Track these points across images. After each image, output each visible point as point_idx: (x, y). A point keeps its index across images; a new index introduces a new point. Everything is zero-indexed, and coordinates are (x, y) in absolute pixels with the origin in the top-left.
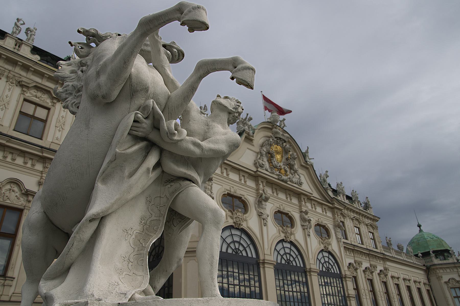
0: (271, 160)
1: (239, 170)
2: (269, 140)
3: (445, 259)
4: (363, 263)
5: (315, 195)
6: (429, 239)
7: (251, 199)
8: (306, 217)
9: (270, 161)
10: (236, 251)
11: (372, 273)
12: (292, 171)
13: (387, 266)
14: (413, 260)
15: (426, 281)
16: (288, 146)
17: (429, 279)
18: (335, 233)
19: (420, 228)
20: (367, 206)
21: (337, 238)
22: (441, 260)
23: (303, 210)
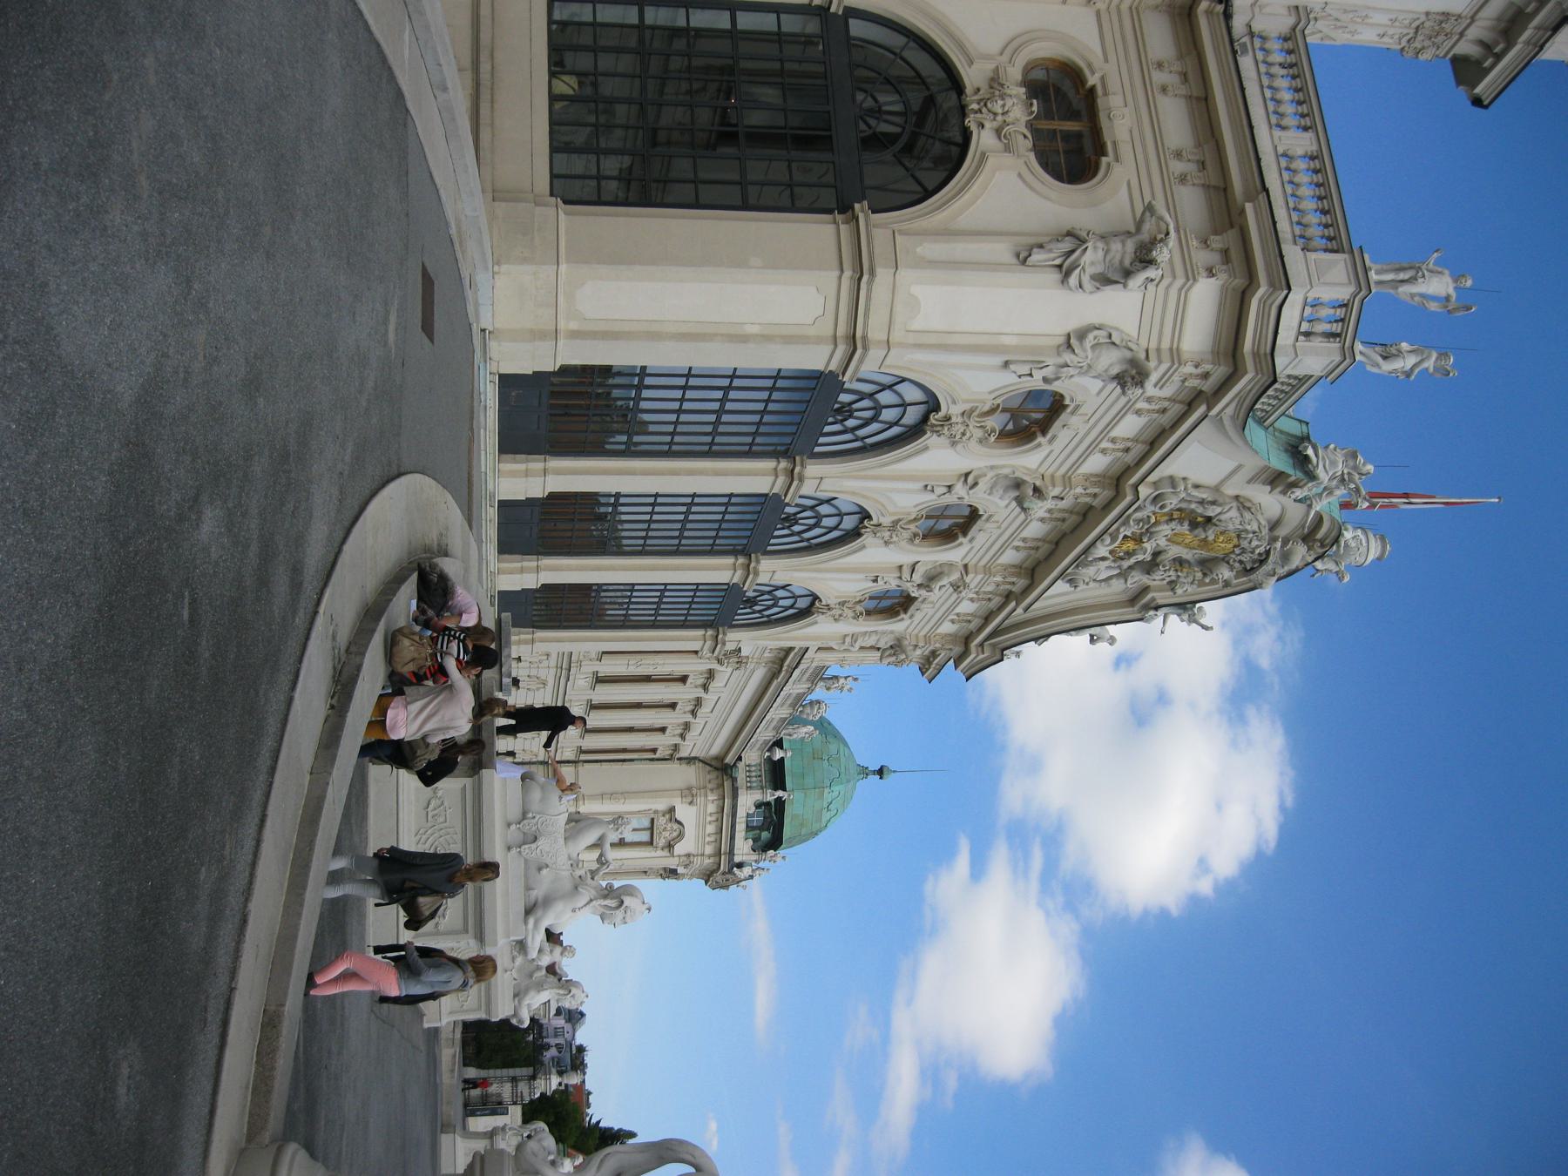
3: (749, 828)
6: (828, 796)
13: (750, 666)
17: (690, 760)
19: (874, 772)
23: (971, 576)
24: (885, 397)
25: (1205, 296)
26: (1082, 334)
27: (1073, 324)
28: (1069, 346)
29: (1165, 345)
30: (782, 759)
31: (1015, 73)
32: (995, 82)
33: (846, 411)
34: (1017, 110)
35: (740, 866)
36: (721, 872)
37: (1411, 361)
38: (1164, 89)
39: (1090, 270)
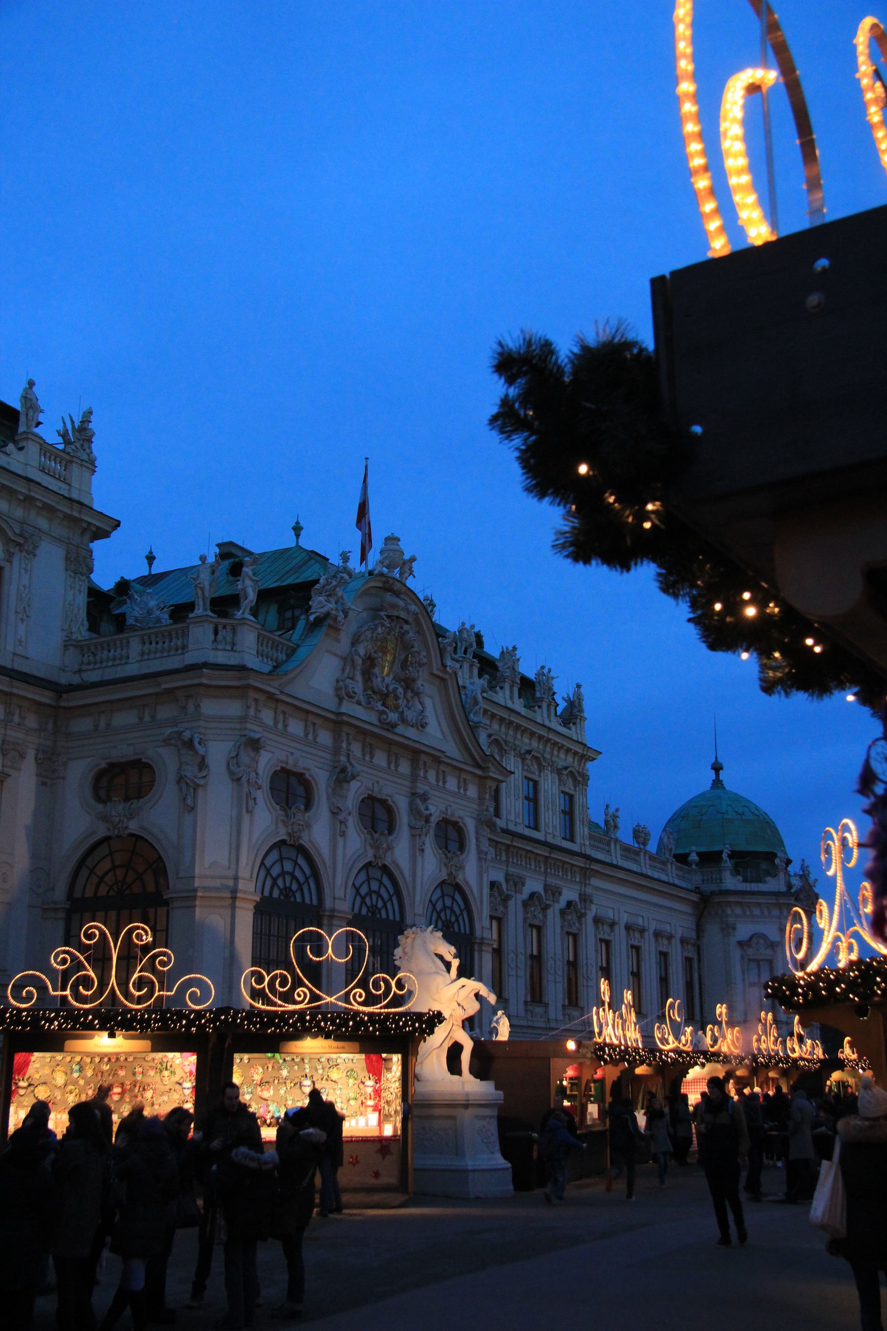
1: (308, 712)
3: (759, 880)
5: (451, 749)
7: (321, 779)
8: (422, 807)
9: (367, 675)
10: (287, 892)
11: (545, 908)
13: (589, 890)
14: (672, 874)
15: (693, 934)
16: (411, 634)
17: (699, 929)
18: (477, 839)
19: (717, 774)
20: (573, 713)
21: (479, 852)
22: (745, 880)
23: (419, 791)
24: (275, 871)
25: (210, 707)
26: (231, 773)
29: (238, 726)
30: (698, 854)
31: (100, 807)
32: (105, 818)
34: (117, 809)
35: (789, 886)
37: (248, 582)
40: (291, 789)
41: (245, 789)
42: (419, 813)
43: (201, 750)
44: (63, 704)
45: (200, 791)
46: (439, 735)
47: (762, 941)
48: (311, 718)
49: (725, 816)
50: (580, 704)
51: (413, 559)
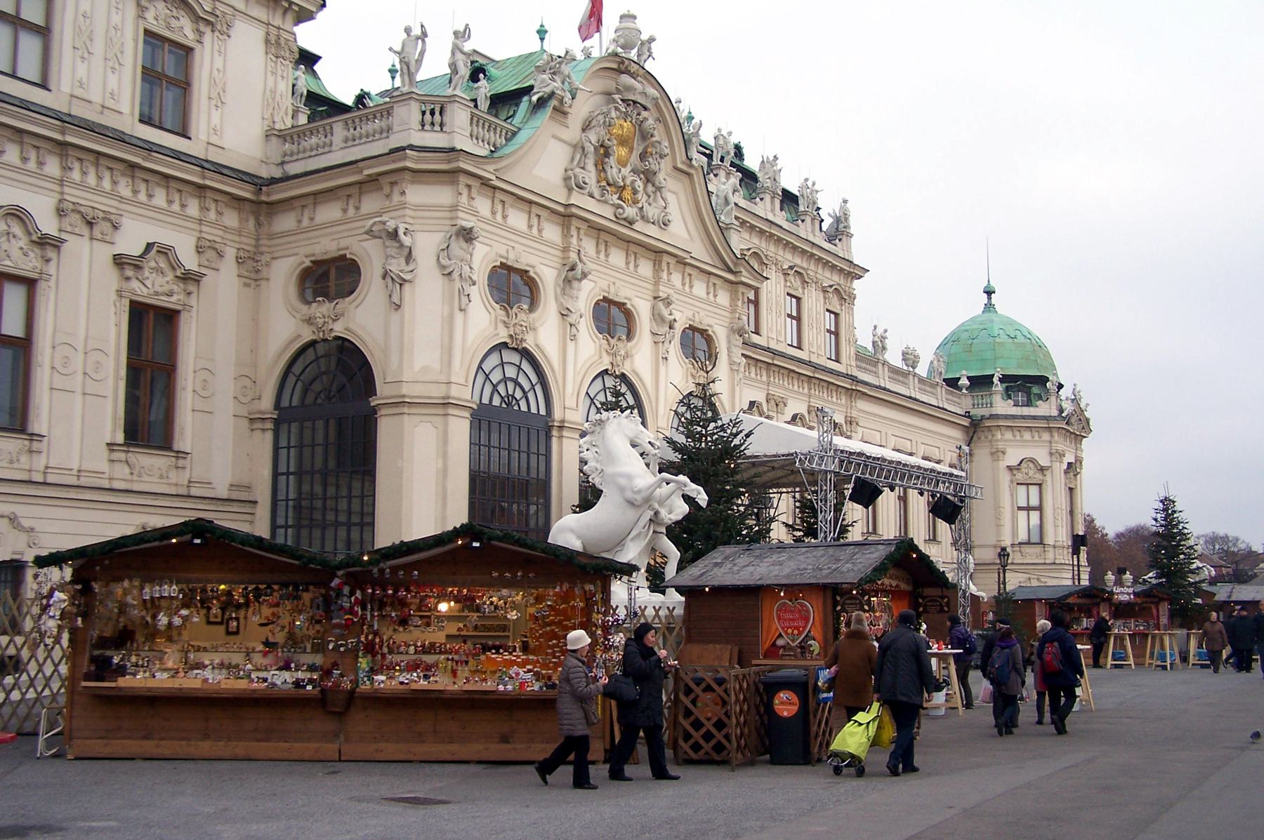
0: (603, 163)
1: (531, 202)
2: (609, 112)
3: (1029, 403)
4: (790, 403)
6: (1004, 338)
7: (547, 275)
8: (665, 312)
9: (601, 166)
10: (509, 400)
12: (650, 188)
13: (854, 414)
16: (651, 121)
18: (729, 349)
19: (989, 298)
20: (839, 231)
21: (732, 363)
23: (660, 294)
24: (496, 377)
25: (417, 194)
27: (437, 273)
28: (450, 274)
29: (448, 215)
31: (304, 308)
32: (309, 321)
33: (509, 400)
34: (322, 309)
35: (1061, 411)
36: (1074, 425)
38: (312, 219)
39: (403, 266)
40: (513, 286)
41: (458, 284)
42: (663, 319)
43: (407, 241)
44: (264, 198)
45: (407, 287)
46: (685, 235)
47: (1031, 465)
48: (535, 210)
49: (997, 340)
50: (846, 219)
51: (652, 40)
